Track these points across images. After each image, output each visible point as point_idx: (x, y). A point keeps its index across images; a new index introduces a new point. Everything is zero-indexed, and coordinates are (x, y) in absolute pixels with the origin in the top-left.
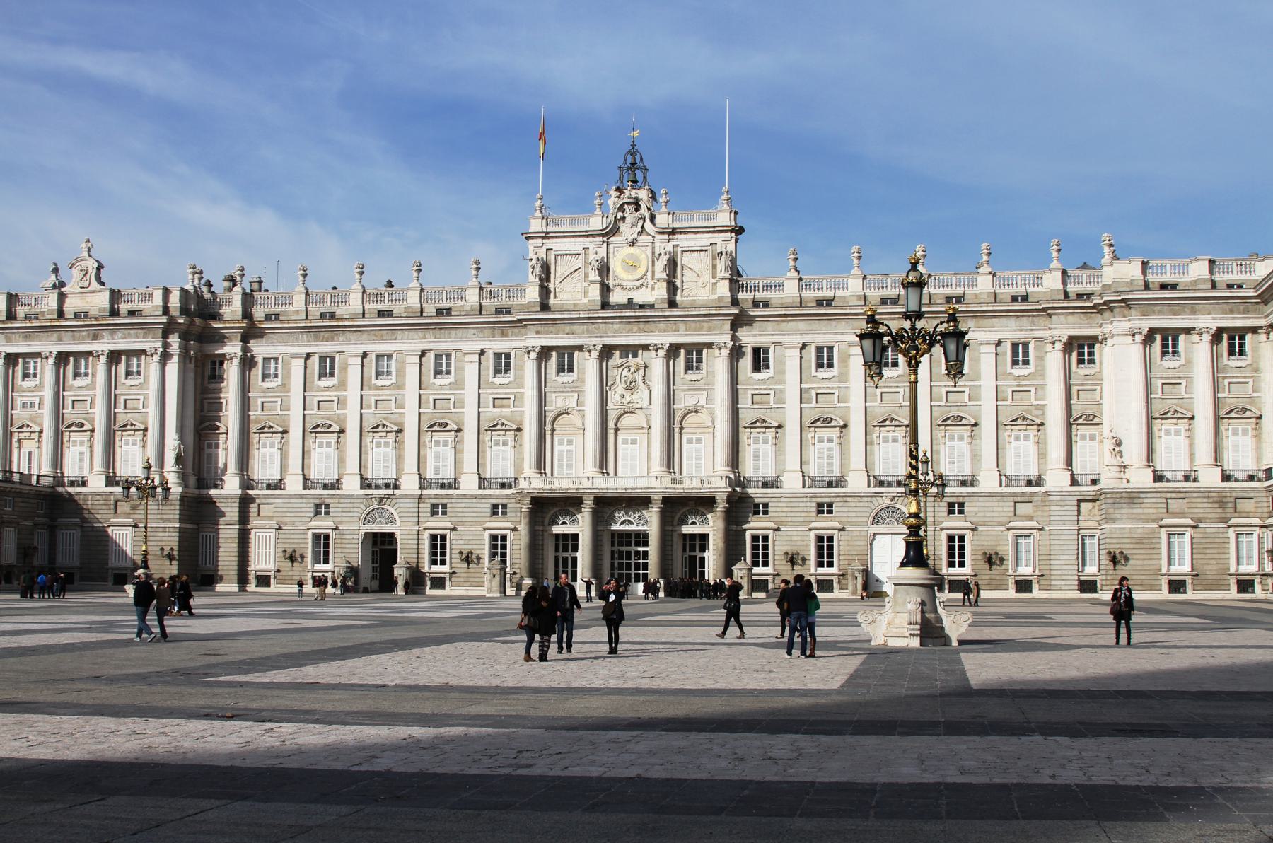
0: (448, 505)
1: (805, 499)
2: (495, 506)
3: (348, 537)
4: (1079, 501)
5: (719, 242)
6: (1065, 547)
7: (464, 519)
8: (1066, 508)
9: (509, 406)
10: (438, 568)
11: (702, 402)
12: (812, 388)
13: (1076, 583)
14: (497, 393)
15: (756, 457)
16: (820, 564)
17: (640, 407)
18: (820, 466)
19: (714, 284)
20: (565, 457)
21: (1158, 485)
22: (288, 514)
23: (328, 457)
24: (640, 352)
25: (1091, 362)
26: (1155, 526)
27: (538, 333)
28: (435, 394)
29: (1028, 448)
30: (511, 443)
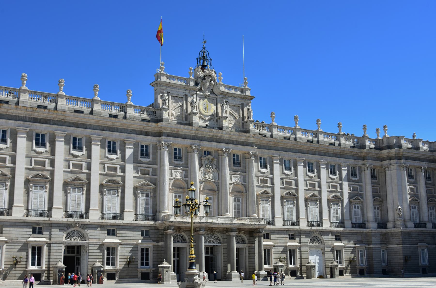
3: (55, 248)
5: (245, 104)
6: (377, 255)
7: (126, 238)
8: (377, 238)
13: (381, 270)
14: (142, 167)
15: (263, 210)
19: (243, 123)
21: (417, 229)
22: (13, 232)
23: (41, 196)
24: (214, 152)
26: (416, 246)
27: (168, 136)
28: (108, 164)
29: (359, 211)
30: (151, 194)
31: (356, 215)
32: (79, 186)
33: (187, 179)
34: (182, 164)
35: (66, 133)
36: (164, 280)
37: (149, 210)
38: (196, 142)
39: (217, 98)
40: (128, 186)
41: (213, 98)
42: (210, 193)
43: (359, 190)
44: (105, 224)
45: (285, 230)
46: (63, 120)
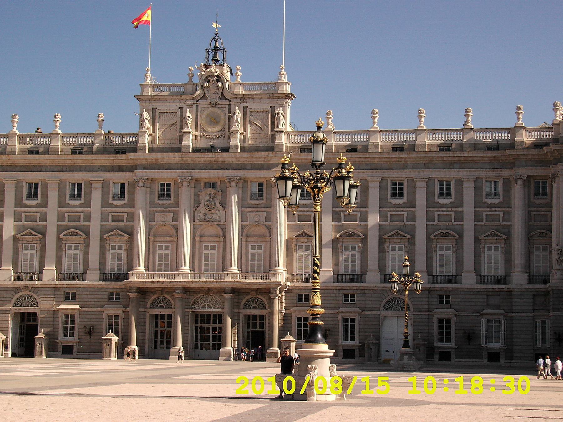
0: (77, 293)
1: (335, 291)
2: (112, 294)
4: (534, 295)
5: (276, 106)
7: (88, 303)
9: (123, 221)
10: (69, 338)
11: (263, 219)
12: (343, 211)
16: (346, 339)
17: (217, 223)
18: (346, 266)
20: (163, 259)
25: (545, 194)
27: (145, 168)
30: (124, 247)
31: (490, 262)
32: (33, 242)
33: (175, 223)
34: (170, 203)
35: (15, 179)
36: (104, 355)
37: (122, 267)
38: (186, 173)
39: (229, 105)
40: (94, 238)
41: (225, 106)
42: (215, 240)
43: (501, 220)
44: (61, 286)
45: (336, 289)
46: (12, 165)
